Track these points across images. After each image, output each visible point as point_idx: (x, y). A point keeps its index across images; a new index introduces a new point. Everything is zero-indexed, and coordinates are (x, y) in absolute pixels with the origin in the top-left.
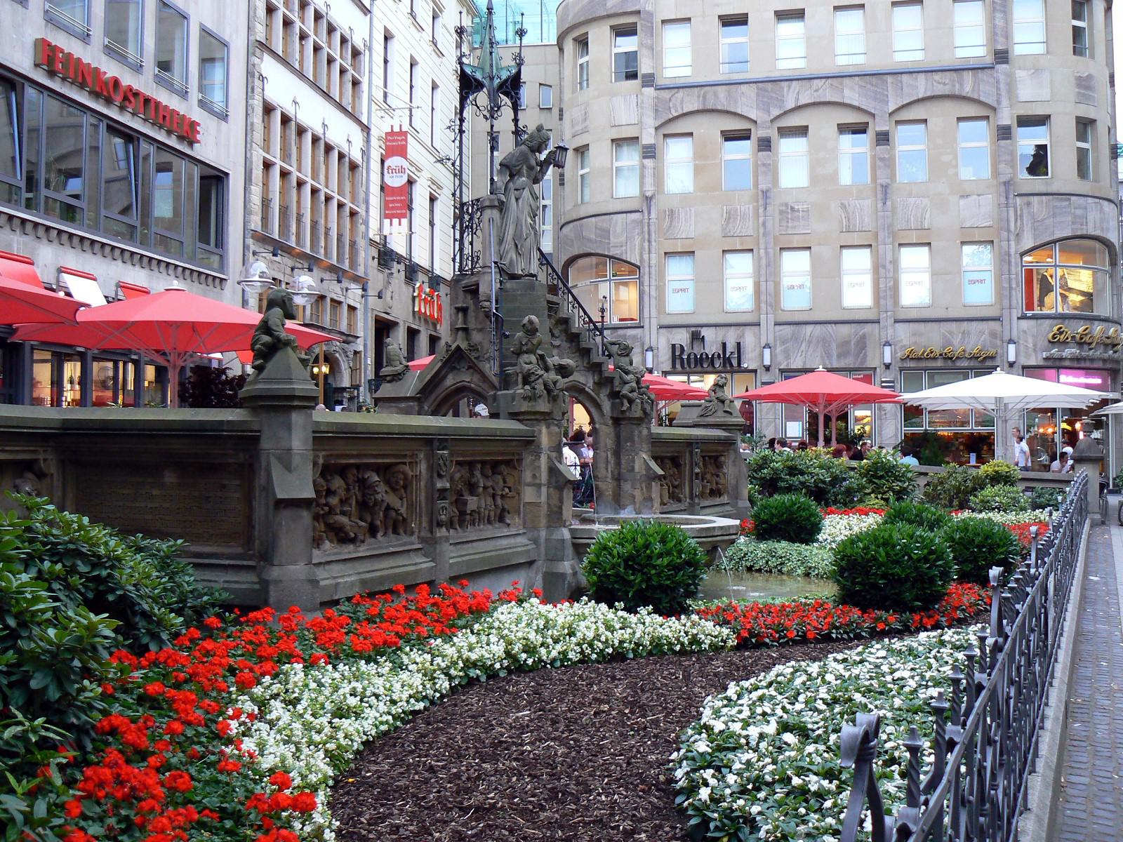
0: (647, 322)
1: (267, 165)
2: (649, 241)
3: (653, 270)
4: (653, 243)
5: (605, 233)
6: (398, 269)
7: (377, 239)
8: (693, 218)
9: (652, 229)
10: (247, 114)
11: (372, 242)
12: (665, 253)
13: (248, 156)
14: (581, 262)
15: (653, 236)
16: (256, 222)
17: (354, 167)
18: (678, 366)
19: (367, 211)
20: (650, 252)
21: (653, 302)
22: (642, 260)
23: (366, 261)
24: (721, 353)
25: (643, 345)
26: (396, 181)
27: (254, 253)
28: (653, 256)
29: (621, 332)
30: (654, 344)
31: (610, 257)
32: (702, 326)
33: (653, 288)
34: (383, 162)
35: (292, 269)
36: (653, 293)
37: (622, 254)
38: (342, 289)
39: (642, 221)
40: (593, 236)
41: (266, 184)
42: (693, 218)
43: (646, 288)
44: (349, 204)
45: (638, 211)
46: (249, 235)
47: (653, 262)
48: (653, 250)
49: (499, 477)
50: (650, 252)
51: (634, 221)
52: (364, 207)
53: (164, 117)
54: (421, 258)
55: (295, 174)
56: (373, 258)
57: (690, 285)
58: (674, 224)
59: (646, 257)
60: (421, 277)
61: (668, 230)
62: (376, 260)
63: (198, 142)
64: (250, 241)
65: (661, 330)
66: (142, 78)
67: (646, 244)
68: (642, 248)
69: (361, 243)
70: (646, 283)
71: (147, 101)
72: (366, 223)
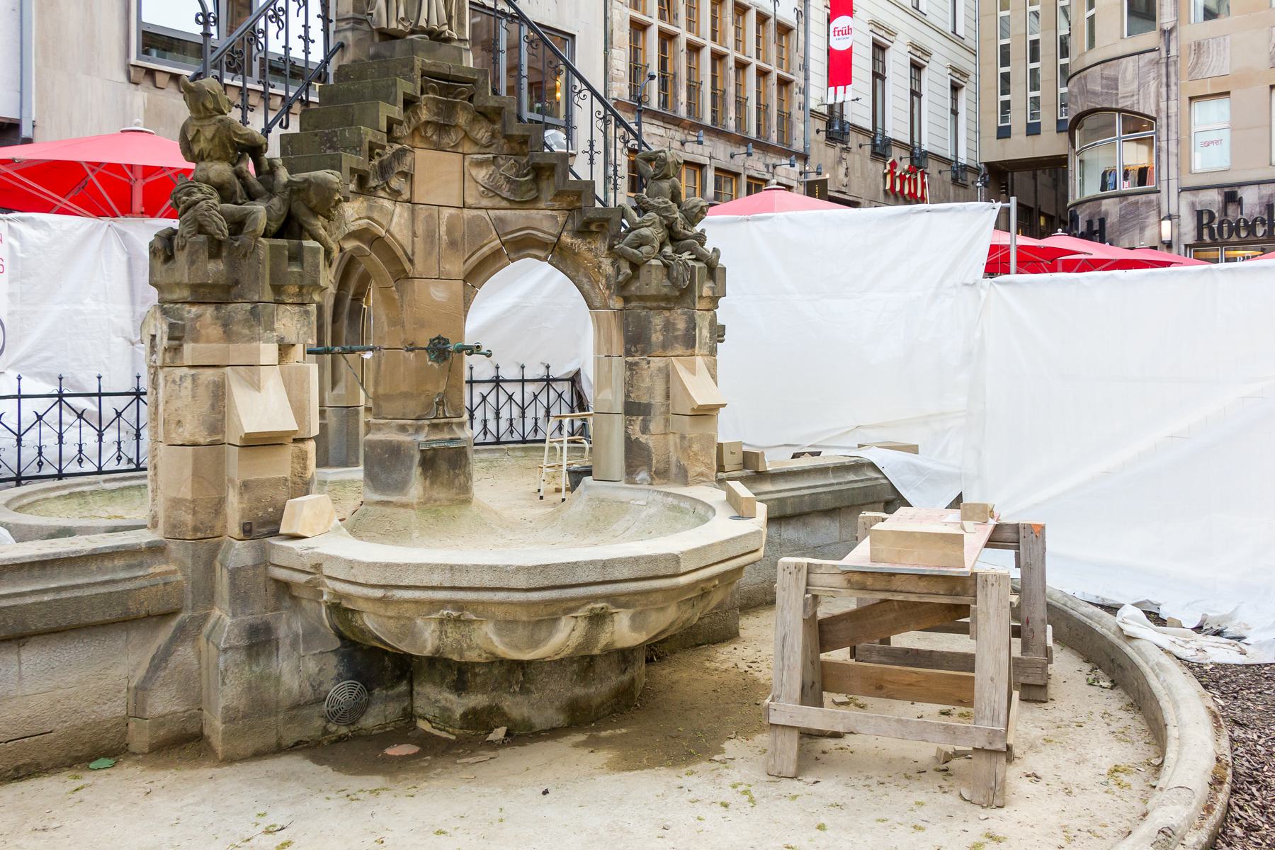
0: (1164, 184)
1: (638, 28)
2: (1168, 86)
3: (1173, 121)
4: (1173, 88)
5: (1113, 83)
6: (859, 145)
7: (824, 110)
8: (1228, 51)
9: (1172, 69)
11: (814, 114)
12: (1191, 99)
13: (609, 15)
14: (1089, 122)
15: (1173, 79)
17: (784, 30)
18: (1206, 238)
19: (806, 79)
20: (1168, 99)
21: (1173, 160)
22: (1158, 111)
23: (806, 133)
24: (1266, 217)
25: (1159, 212)
26: (839, 44)
28: (1173, 103)
29: (1132, 199)
30: (1173, 211)
31: (1119, 111)
32: (1241, 185)
33: (1173, 144)
34: (829, 21)
35: (683, 144)
36: (1173, 148)
37: (1133, 105)
38: (767, 166)
39: (1158, 62)
40: (1098, 88)
41: (635, 52)
42: (1228, 51)
43: (1164, 144)
44: (775, 71)
45: (1153, 50)
47: (1173, 110)
48: (1173, 96)
50: (1168, 99)
51: (1151, 62)
52: (802, 74)
54: (897, 128)
55: (684, 36)
56: (818, 131)
57: (1226, 135)
58: (1201, 60)
59: (1163, 105)
60: (896, 153)
61: (1193, 69)
62: (823, 135)
65: (1183, 194)
67: (1164, 90)
68: (1158, 95)
69: (797, 115)
70: (1164, 138)
72: (804, 92)
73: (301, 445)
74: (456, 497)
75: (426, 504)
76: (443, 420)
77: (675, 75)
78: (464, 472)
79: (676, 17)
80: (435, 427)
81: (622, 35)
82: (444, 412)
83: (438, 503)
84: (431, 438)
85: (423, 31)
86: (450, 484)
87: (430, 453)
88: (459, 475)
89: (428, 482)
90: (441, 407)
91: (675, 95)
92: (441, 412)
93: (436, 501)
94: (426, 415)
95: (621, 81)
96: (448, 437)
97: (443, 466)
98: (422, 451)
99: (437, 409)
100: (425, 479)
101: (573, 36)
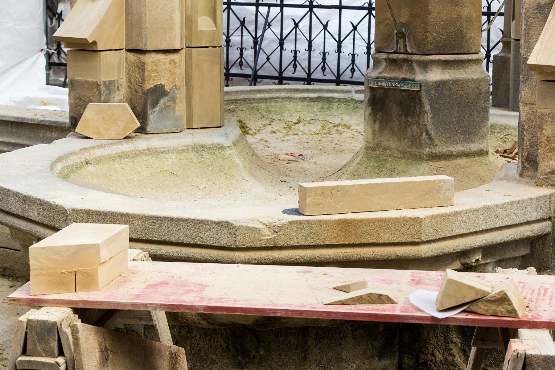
73: (141, 56)
74: (409, 150)
75: (374, 149)
76: (401, 56)
78: (418, 122)
80: (392, 62)
82: (405, 46)
83: (388, 152)
84: (386, 75)
86: (401, 133)
87: (380, 92)
88: (412, 123)
89: (377, 126)
90: (401, 41)
92: (401, 45)
93: (385, 149)
94: (386, 47)
96: (401, 75)
97: (395, 110)
98: (372, 88)
99: (398, 42)
100: (375, 121)
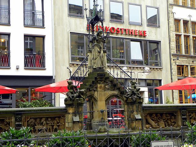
10: (168, 24)
16: (174, 51)
27: (174, 60)
35: (193, 62)
46: (171, 55)
49: (55, 121)
53: (132, 33)
63: (146, 36)
64: (172, 57)
66: (124, 25)
71: (125, 30)
77: (189, 45)
79: (189, 31)
81: (173, 38)
85: (98, 68)
91: (190, 50)
95: (174, 49)
101: (160, 41)
